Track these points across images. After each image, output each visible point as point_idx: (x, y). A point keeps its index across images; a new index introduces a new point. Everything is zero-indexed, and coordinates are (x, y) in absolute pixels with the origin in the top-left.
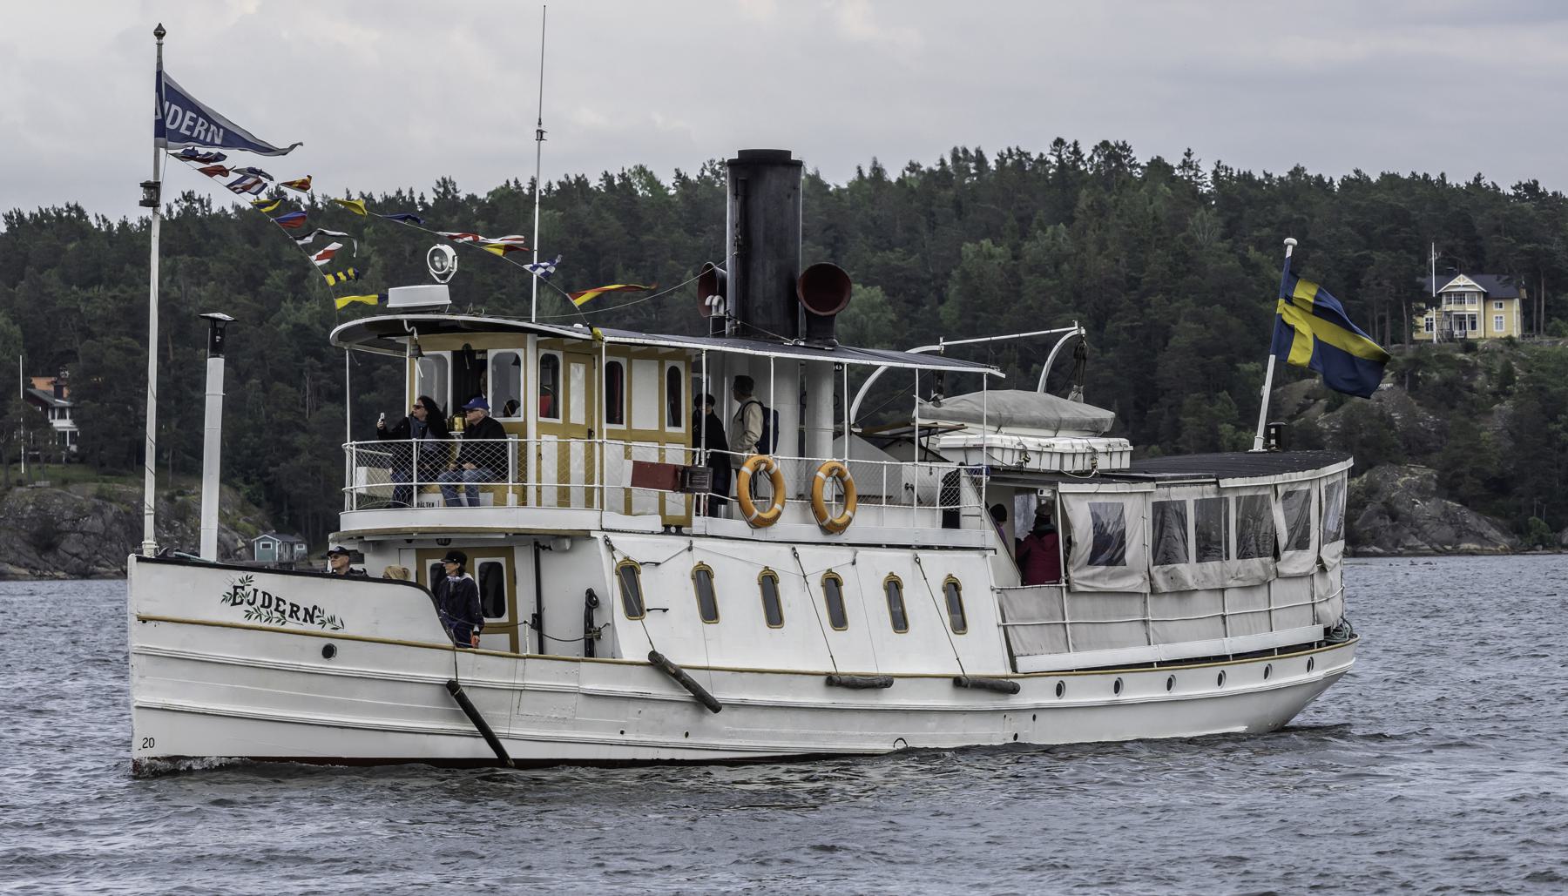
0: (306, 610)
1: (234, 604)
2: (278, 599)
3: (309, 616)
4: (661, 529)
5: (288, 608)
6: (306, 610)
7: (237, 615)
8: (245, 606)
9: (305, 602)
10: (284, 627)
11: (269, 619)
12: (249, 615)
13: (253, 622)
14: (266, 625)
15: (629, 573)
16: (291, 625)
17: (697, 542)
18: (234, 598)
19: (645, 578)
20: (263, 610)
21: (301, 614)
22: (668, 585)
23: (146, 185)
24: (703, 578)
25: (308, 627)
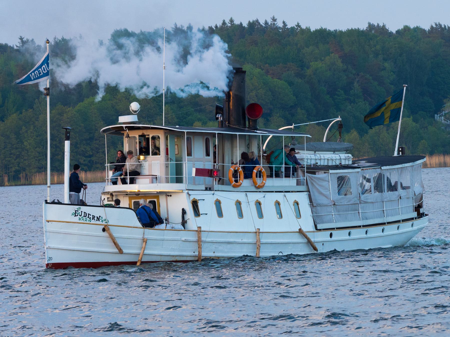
0: (97, 217)
1: (75, 216)
2: (89, 214)
3: (98, 219)
4: (204, 189)
6: (97, 217)
7: (76, 219)
8: (79, 216)
12: (80, 219)
13: (82, 221)
14: (85, 222)
16: (93, 221)
18: (75, 214)
19: (200, 204)
21: (96, 218)
24: (218, 203)
25: (98, 222)
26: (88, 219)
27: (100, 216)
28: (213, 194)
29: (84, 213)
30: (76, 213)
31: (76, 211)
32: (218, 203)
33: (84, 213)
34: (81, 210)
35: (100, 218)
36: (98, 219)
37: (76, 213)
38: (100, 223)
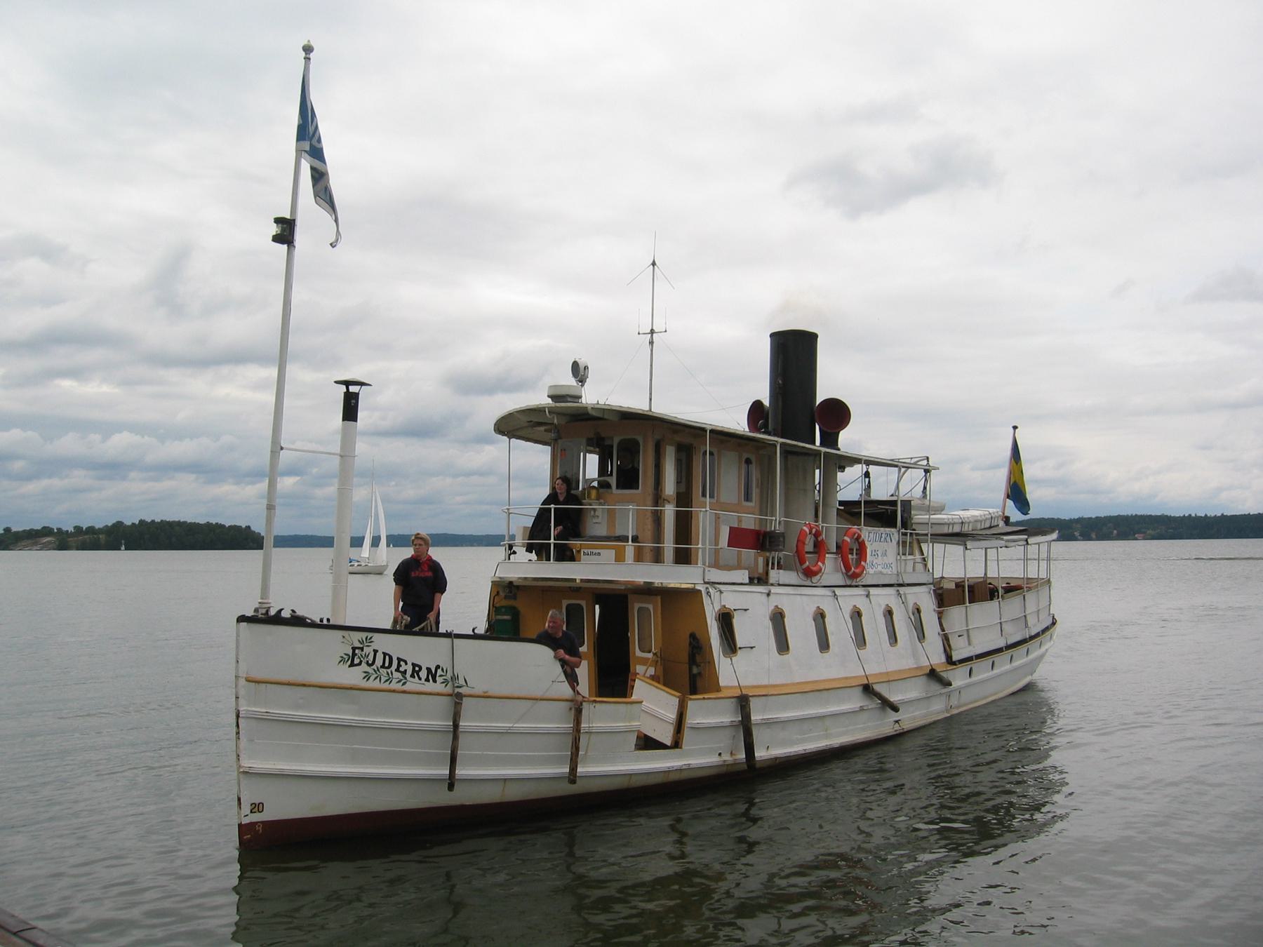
0: (429, 670)
1: (352, 665)
2: (399, 660)
3: (432, 675)
5: (410, 669)
6: (429, 670)
7: (354, 676)
8: (364, 667)
9: (427, 662)
10: (406, 688)
11: (389, 680)
12: (367, 676)
13: (373, 684)
14: (386, 686)
15: (726, 619)
17: (774, 590)
18: (352, 660)
19: (737, 622)
20: (383, 671)
21: (423, 674)
22: (752, 628)
23: (278, 221)
24: (778, 618)
25: (430, 687)
26: (399, 675)
27: (438, 667)
28: (768, 595)
29: (385, 654)
30: (354, 654)
31: (354, 649)
32: (778, 618)
33: (385, 654)
34: (374, 646)
35: (439, 672)
36: (432, 675)
37: (354, 654)
38: (438, 687)
